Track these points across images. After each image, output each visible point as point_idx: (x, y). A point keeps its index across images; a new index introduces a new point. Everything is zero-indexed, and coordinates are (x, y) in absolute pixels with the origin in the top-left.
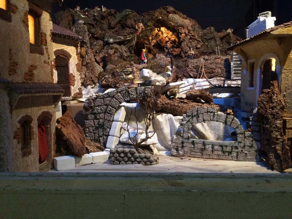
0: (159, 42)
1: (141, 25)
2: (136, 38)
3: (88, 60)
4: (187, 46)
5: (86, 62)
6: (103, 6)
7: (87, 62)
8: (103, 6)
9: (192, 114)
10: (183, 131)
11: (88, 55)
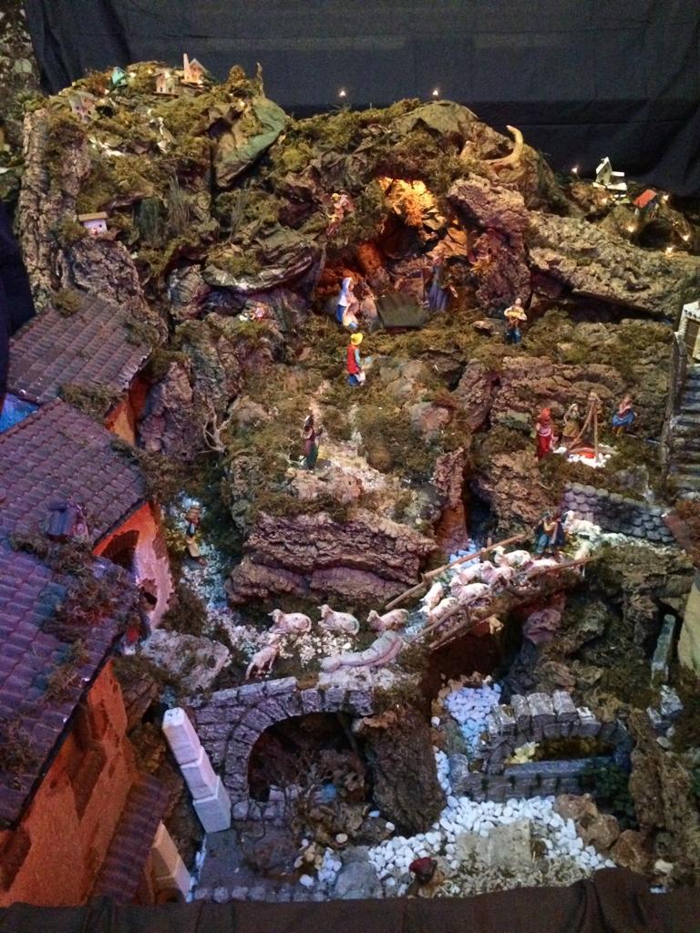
0: (399, 212)
1: (342, 200)
2: (324, 256)
3: (168, 401)
4: (503, 276)
5: (161, 408)
6: (185, 56)
7: (165, 408)
8: (185, 56)
9: (516, 730)
10: (488, 762)
11: (167, 386)
